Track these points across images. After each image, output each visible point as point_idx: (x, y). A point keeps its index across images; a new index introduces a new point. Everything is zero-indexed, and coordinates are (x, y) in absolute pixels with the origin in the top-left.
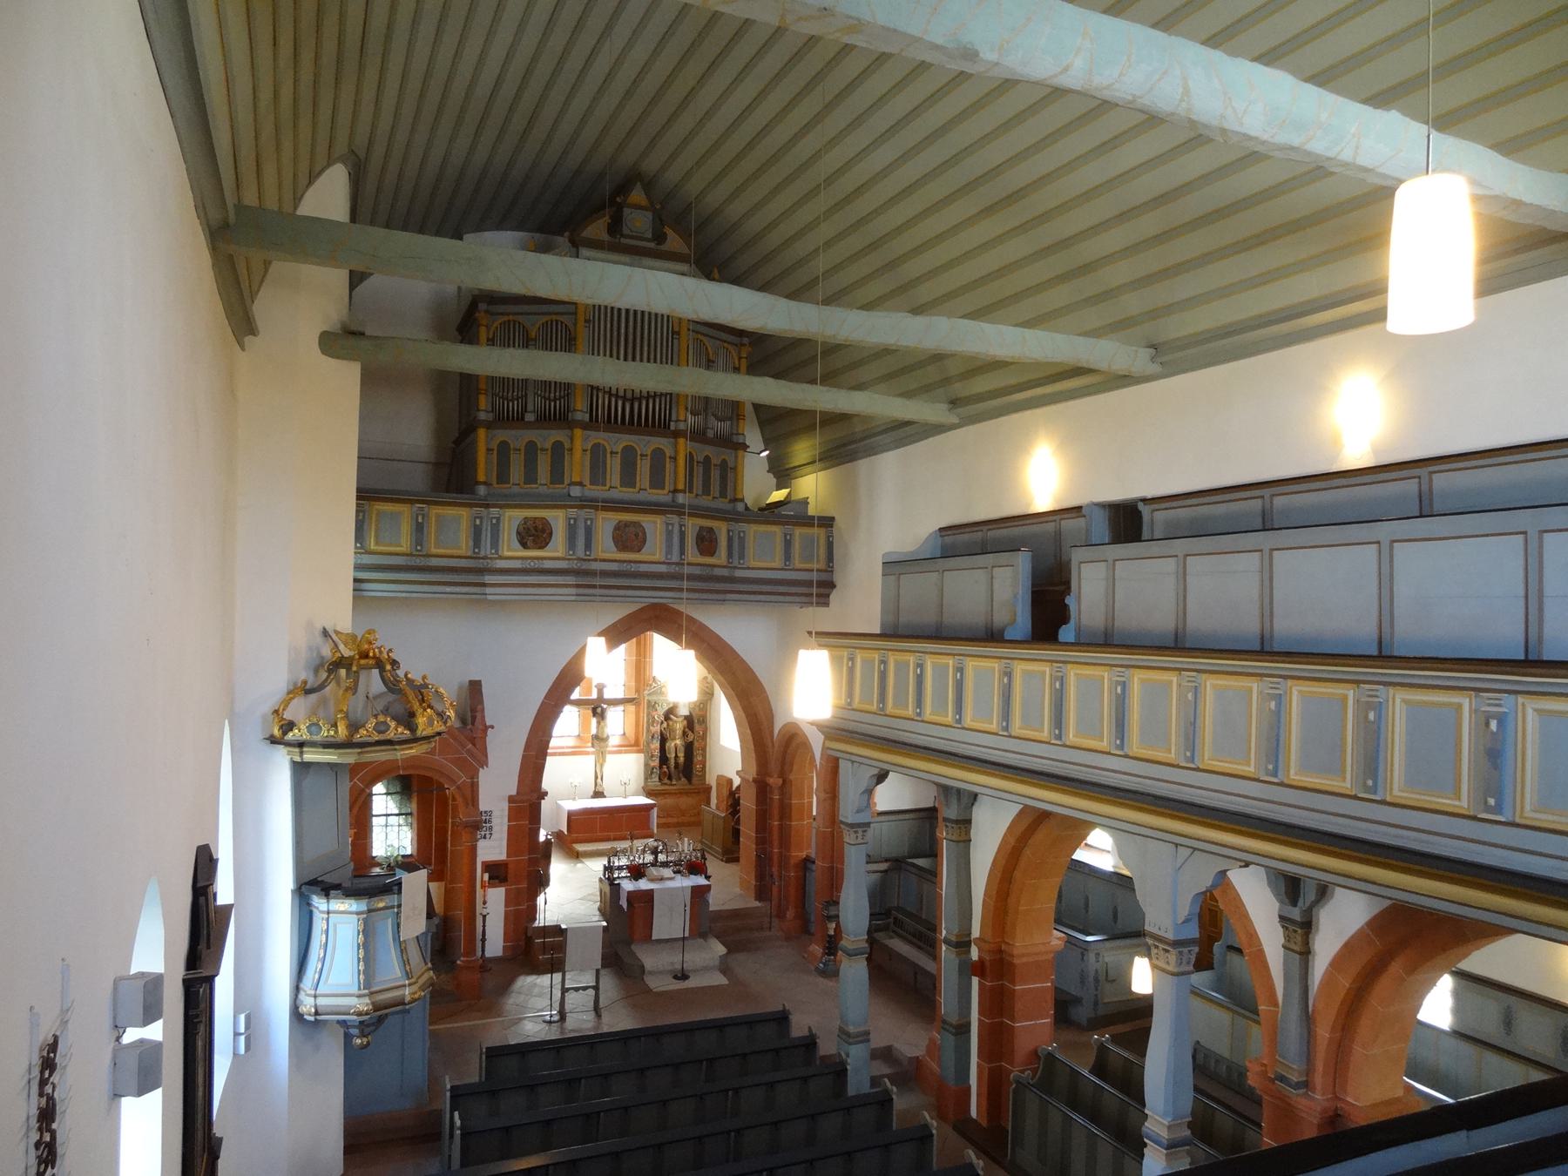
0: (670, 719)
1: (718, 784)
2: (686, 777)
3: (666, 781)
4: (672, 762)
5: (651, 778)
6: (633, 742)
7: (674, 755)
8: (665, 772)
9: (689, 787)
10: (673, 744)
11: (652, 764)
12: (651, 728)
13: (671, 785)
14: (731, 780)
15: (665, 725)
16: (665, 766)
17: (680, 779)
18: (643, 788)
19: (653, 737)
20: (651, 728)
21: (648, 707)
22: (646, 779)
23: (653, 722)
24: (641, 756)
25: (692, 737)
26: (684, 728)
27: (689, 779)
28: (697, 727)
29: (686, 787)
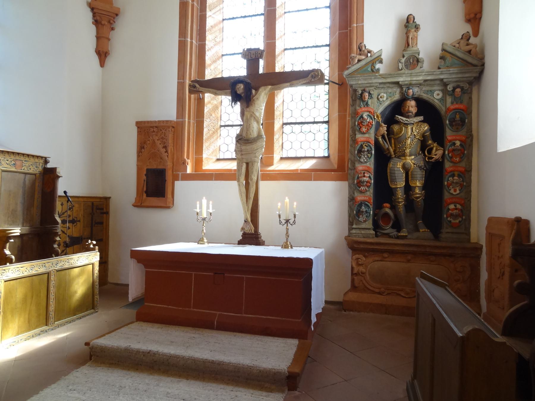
0: (398, 122)
1: (490, 236)
2: (428, 226)
3: (388, 229)
4: (400, 194)
5: (359, 222)
6: (336, 166)
7: (401, 184)
8: (386, 214)
9: (438, 244)
10: (399, 165)
11: (360, 198)
12: (359, 136)
13: (398, 237)
14: (527, 223)
15: (384, 129)
16: (388, 205)
17: (417, 229)
18: (346, 238)
19: (360, 151)
20: (359, 136)
21: (354, 101)
22: (351, 223)
23: (361, 124)
24: (345, 185)
25: (440, 152)
26: (423, 136)
27: (436, 232)
28: (449, 134)
29: (432, 243)
